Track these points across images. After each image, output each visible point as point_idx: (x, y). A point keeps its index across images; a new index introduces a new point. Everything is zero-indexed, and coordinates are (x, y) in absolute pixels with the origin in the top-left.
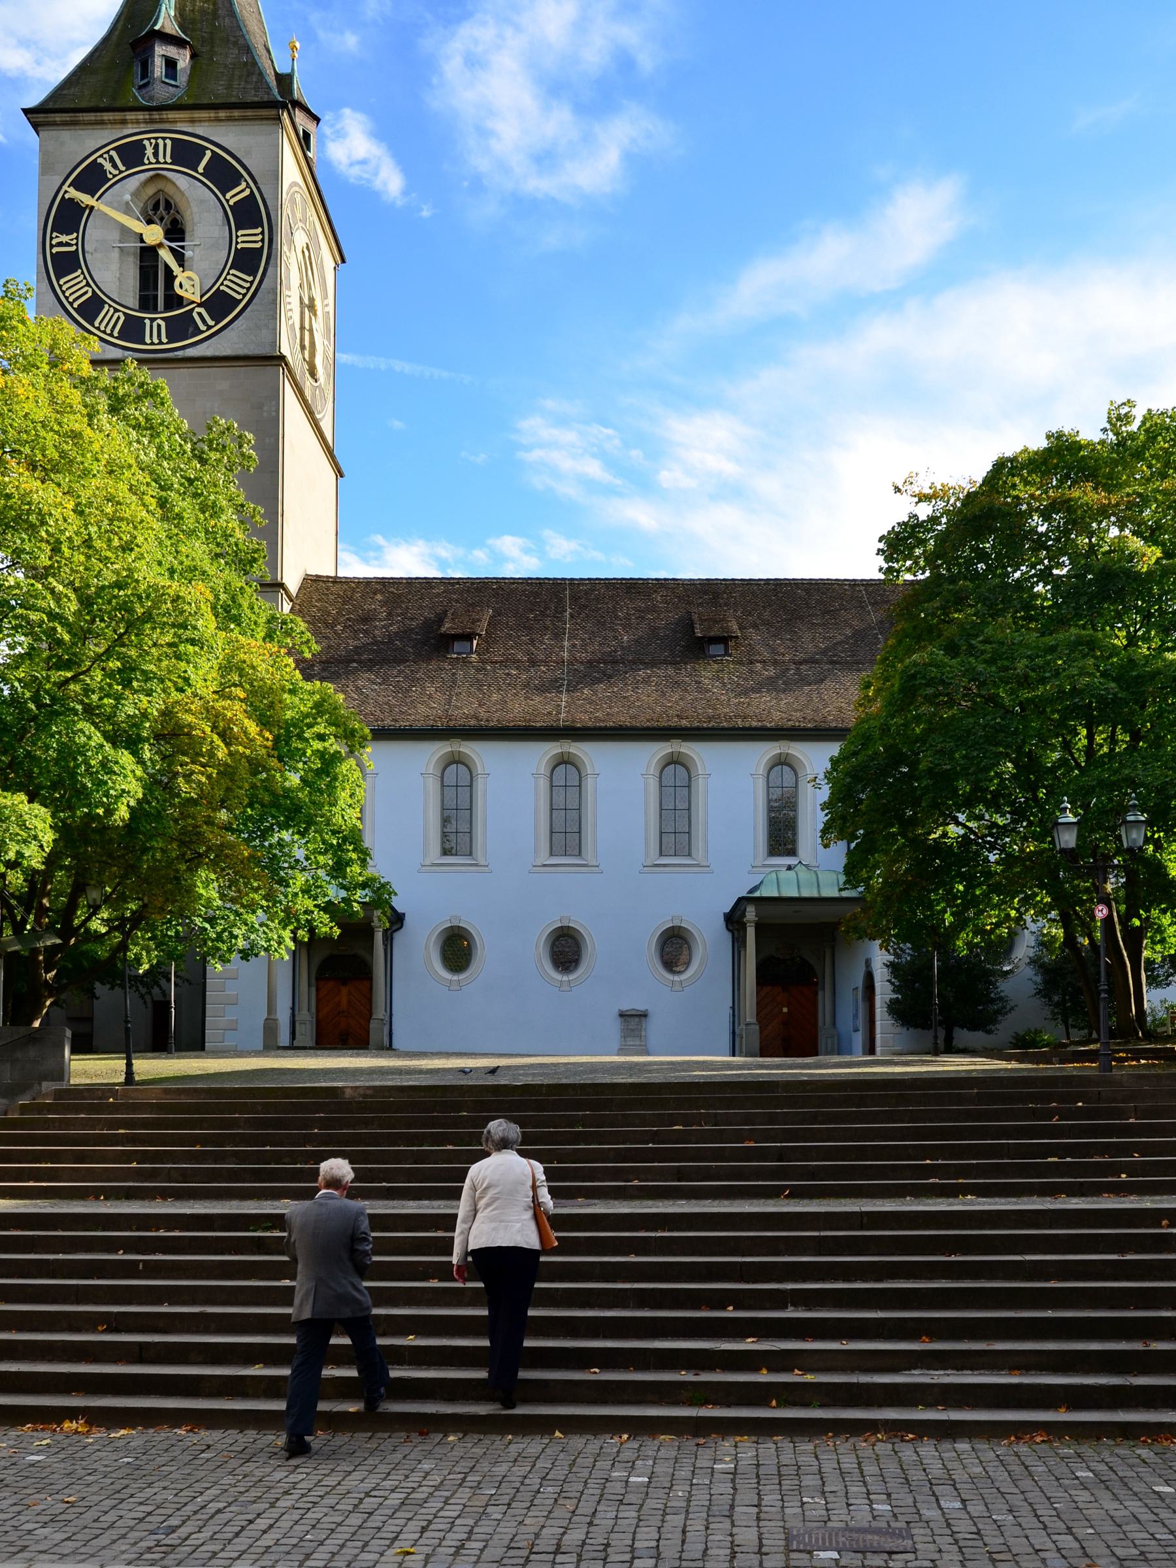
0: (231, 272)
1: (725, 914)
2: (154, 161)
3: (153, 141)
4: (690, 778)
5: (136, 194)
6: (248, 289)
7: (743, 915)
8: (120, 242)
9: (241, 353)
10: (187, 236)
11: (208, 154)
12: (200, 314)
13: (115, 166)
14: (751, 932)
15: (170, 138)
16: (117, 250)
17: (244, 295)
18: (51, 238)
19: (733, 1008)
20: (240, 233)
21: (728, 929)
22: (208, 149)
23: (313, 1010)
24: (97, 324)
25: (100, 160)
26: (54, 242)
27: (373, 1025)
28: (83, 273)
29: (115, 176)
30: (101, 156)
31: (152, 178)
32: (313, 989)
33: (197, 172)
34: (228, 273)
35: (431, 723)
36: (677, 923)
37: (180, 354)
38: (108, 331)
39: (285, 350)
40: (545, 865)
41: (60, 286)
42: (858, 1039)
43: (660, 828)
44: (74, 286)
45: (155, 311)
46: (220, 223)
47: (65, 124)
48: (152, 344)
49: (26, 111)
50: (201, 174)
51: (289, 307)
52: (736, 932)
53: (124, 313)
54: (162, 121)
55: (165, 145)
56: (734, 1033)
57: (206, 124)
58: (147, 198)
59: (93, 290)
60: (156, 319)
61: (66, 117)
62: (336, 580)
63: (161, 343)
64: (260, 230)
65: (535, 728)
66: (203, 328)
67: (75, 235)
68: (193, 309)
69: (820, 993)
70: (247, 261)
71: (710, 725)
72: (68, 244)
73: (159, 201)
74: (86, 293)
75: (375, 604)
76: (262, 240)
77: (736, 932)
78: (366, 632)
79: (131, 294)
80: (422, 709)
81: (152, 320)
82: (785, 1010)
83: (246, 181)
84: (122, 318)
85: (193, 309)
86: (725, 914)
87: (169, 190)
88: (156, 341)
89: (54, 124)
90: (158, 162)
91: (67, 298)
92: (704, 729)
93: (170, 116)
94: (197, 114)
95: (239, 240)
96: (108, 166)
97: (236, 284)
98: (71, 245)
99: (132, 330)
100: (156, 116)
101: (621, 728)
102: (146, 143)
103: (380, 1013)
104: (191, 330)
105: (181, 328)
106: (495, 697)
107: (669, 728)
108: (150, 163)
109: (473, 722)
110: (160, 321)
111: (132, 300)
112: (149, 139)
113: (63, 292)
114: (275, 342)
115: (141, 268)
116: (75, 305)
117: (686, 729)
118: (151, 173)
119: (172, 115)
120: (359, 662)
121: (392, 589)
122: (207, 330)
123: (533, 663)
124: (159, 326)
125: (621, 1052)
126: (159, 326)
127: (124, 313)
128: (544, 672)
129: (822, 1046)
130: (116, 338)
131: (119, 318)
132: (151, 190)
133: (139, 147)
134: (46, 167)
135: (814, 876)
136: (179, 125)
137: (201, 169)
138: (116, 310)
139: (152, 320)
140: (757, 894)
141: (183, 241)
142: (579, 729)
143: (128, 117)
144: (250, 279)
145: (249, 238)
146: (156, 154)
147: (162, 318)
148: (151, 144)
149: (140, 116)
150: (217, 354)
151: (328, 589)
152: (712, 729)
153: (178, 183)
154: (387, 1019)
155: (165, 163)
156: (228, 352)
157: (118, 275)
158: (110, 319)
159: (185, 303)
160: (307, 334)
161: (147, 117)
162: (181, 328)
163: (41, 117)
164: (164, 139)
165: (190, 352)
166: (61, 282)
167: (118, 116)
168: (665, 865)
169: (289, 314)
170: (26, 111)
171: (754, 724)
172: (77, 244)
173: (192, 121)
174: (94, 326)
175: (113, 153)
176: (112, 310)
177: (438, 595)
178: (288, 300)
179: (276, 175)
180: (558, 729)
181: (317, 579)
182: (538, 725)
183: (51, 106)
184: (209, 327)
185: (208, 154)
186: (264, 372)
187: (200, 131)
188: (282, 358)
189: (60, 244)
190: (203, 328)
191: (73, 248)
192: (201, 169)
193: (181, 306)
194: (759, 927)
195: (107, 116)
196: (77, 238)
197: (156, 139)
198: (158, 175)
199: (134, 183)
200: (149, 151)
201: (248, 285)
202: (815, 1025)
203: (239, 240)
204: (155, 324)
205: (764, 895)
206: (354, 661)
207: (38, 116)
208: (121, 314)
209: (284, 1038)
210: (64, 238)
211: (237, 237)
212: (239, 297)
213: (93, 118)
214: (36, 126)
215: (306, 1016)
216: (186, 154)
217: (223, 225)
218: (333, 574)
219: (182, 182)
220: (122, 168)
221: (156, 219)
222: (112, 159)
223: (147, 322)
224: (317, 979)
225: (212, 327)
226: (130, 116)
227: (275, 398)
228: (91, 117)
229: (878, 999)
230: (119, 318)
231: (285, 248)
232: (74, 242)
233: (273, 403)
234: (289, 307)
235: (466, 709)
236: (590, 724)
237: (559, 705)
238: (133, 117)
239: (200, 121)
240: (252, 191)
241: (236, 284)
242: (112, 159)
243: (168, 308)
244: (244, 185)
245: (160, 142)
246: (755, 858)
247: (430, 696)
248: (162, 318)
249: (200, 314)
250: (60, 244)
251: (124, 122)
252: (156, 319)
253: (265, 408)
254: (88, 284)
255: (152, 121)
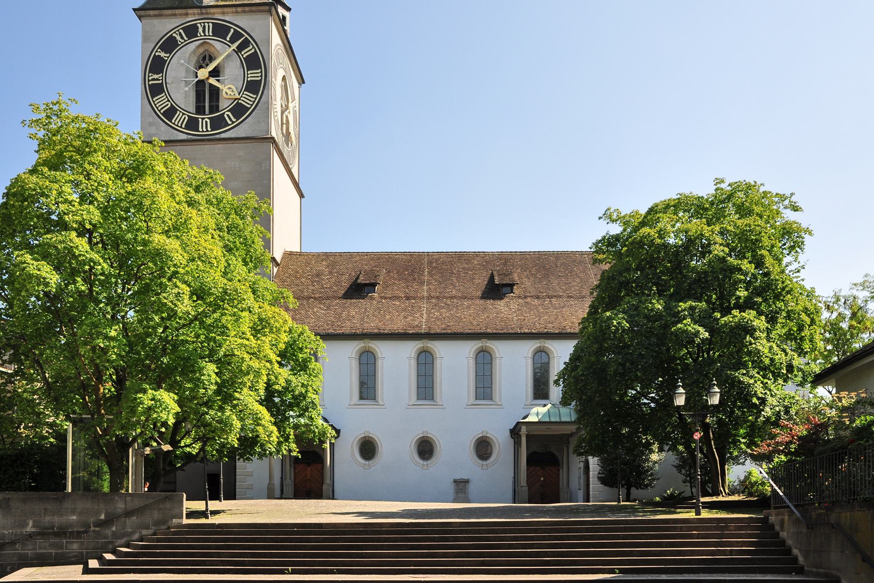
0: (245, 93)
1: (510, 430)
2: (203, 34)
3: (202, 24)
4: (492, 359)
5: (194, 52)
6: (254, 102)
7: (520, 430)
8: (185, 78)
9: (250, 135)
10: (221, 75)
11: (232, 31)
12: (228, 115)
13: (182, 38)
14: (524, 440)
15: (211, 23)
16: (183, 82)
17: (252, 105)
18: (149, 76)
19: (514, 478)
20: (249, 72)
21: (512, 437)
22: (232, 28)
23: (293, 479)
24: (173, 121)
25: (174, 35)
26: (150, 78)
27: (325, 487)
28: (165, 94)
29: (182, 43)
30: (175, 33)
31: (202, 44)
32: (292, 469)
33: (226, 40)
34: (243, 94)
35: (354, 331)
36: (485, 434)
37: (218, 136)
38: (179, 125)
39: (274, 134)
40: (414, 405)
41: (154, 102)
42: (581, 494)
43: (476, 385)
44: (162, 102)
45: (204, 114)
46: (239, 67)
47: (155, 16)
48: (203, 131)
49: (134, 10)
50: (228, 41)
51: (275, 110)
52: (516, 439)
53: (188, 115)
54: (207, 13)
55: (209, 26)
56: (515, 491)
57: (231, 14)
58: (199, 54)
59: (171, 104)
60: (205, 118)
61: (156, 12)
62: (300, 254)
63: (207, 131)
64: (260, 70)
65: (409, 334)
66: (230, 122)
67: (161, 74)
68: (225, 113)
69: (561, 470)
70: (253, 87)
71: (502, 332)
72: (157, 79)
73: (205, 56)
74: (168, 105)
75: (323, 267)
76: (261, 76)
77: (516, 439)
78: (318, 282)
79: (192, 105)
80: (348, 324)
81: (203, 119)
82: (542, 479)
83: (252, 44)
84: (187, 118)
85: (225, 113)
86: (510, 430)
87: (212, 50)
88: (205, 130)
89: (150, 16)
90: (205, 35)
91: (157, 108)
92: (499, 334)
93: (211, 11)
94: (226, 10)
95: (249, 76)
96: (178, 38)
97: (247, 99)
98: (159, 80)
99: (192, 124)
100: (204, 11)
101: (455, 334)
102: (199, 25)
103: (328, 481)
104: (223, 124)
105: (218, 123)
106: (387, 317)
107: (481, 334)
108: (201, 36)
109: (376, 331)
110: (207, 119)
111: (192, 109)
112: (200, 23)
113: (155, 105)
114: (268, 130)
115: (196, 91)
116: (162, 112)
117: (490, 334)
118: (202, 41)
119: (212, 10)
120: (315, 298)
121: (331, 259)
122: (232, 124)
123: (408, 298)
124: (206, 122)
125: (455, 501)
126: (206, 122)
127: (188, 115)
128: (414, 303)
129: (562, 495)
130: (183, 128)
131: (185, 118)
132: (201, 50)
133: (195, 27)
134: (145, 39)
135: (557, 410)
136: (216, 15)
137: (228, 39)
138: (183, 114)
139: (203, 119)
140: (526, 420)
141: (219, 77)
142: (432, 334)
143: (189, 12)
144: (255, 96)
145: (254, 75)
146: (204, 31)
147: (208, 118)
148: (201, 25)
149: (196, 11)
150: (237, 136)
151: (297, 259)
152: (504, 334)
153: (215, 46)
154: (332, 483)
155: (209, 35)
156: (243, 135)
157: (184, 95)
158: (180, 119)
159: (220, 109)
160: (284, 126)
161: (199, 12)
162: (218, 123)
163: (142, 13)
164: (208, 23)
165: (223, 136)
166: (154, 100)
167: (184, 11)
168: (478, 405)
169: (276, 114)
170: (134, 10)
171: (526, 331)
172: (162, 79)
173: (223, 13)
174: (172, 123)
175: (181, 31)
176: (181, 114)
177: (356, 262)
178: (275, 106)
179: (268, 41)
180: (421, 334)
181: (291, 254)
182: (411, 332)
183: (148, 6)
184: (233, 122)
185: (232, 31)
186: (264, 145)
187: (227, 18)
188: (273, 138)
189: (153, 79)
190: (230, 122)
191: (160, 82)
192: (228, 39)
193: (218, 111)
194: (528, 436)
195: (178, 11)
196: (162, 76)
197: (204, 23)
198: (205, 42)
199: (193, 46)
200: (201, 30)
201: (253, 100)
202: (558, 486)
203: (249, 76)
204: (204, 121)
205: (531, 420)
206: (312, 298)
207: (141, 12)
208: (186, 116)
209: (278, 492)
210: (156, 76)
211: (248, 74)
212: (249, 106)
213: (170, 13)
214: (140, 17)
215: (289, 482)
216: (220, 31)
217: (240, 68)
218: (299, 251)
219: (218, 45)
220: (186, 39)
221: (204, 65)
222: (180, 34)
223: (200, 120)
224: (294, 463)
225: (235, 122)
226: (190, 11)
227: (268, 159)
228: (169, 12)
229: (591, 473)
230: (185, 118)
231: (273, 79)
232: (161, 78)
233: (268, 162)
234: (275, 110)
235: (372, 325)
236: (438, 331)
237: (421, 321)
238: (192, 12)
239: (228, 13)
240: (255, 50)
241: (247, 99)
242: (180, 34)
243: (211, 112)
244: (251, 47)
245: (206, 24)
246: (527, 400)
247: (353, 317)
248: (208, 118)
249: (228, 115)
250: (153, 79)
251: (187, 14)
252: (205, 118)
253: (263, 165)
254: (168, 101)
255: (202, 14)
